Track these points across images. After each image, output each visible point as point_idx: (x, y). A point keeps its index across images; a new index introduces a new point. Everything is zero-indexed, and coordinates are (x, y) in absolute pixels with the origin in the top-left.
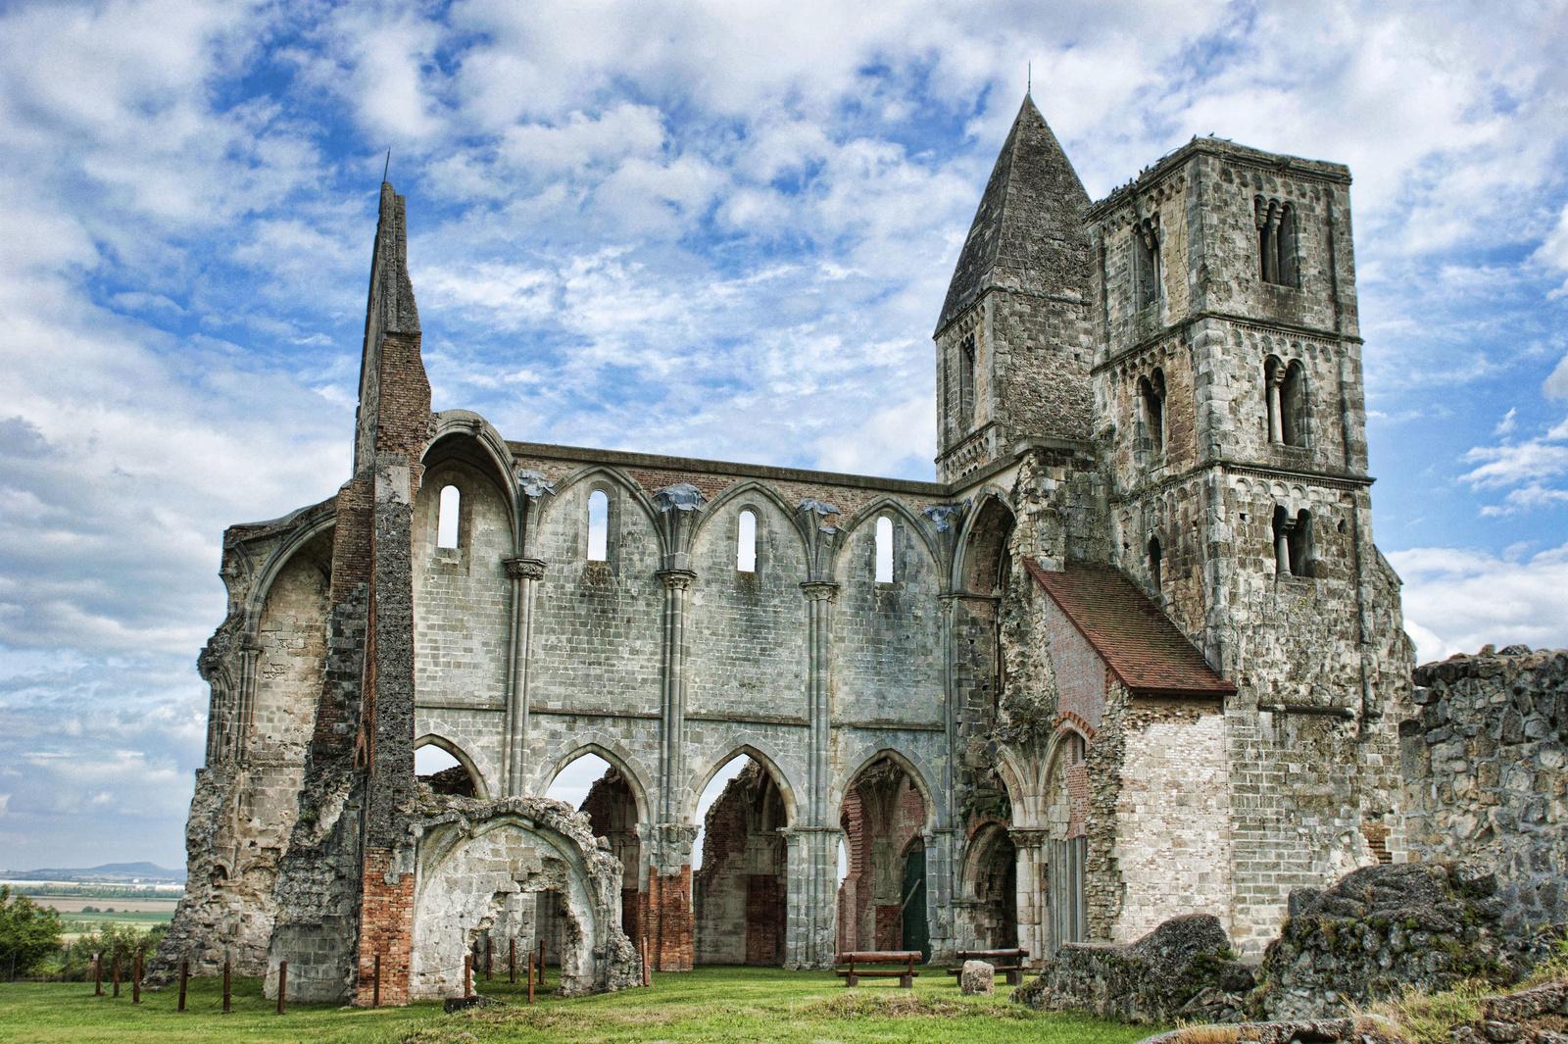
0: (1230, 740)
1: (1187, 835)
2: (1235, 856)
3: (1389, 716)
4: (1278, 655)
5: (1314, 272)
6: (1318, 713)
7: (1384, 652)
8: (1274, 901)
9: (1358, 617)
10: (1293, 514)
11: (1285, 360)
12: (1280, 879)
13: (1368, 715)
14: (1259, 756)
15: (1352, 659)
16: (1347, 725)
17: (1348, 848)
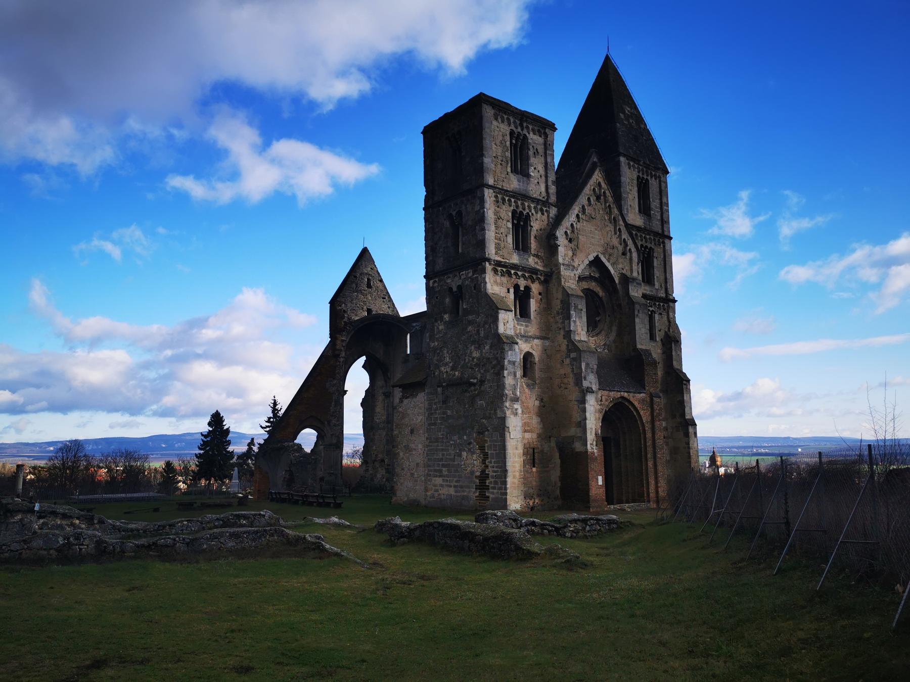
0: (427, 403)
1: (412, 446)
2: (427, 455)
3: (489, 380)
4: (448, 359)
5: (468, 160)
6: (463, 384)
7: (487, 347)
8: (440, 476)
9: (478, 331)
10: (455, 289)
11: (454, 213)
12: (443, 466)
13: (482, 382)
14: (436, 409)
15: (476, 354)
16: (473, 388)
17: (470, 450)
